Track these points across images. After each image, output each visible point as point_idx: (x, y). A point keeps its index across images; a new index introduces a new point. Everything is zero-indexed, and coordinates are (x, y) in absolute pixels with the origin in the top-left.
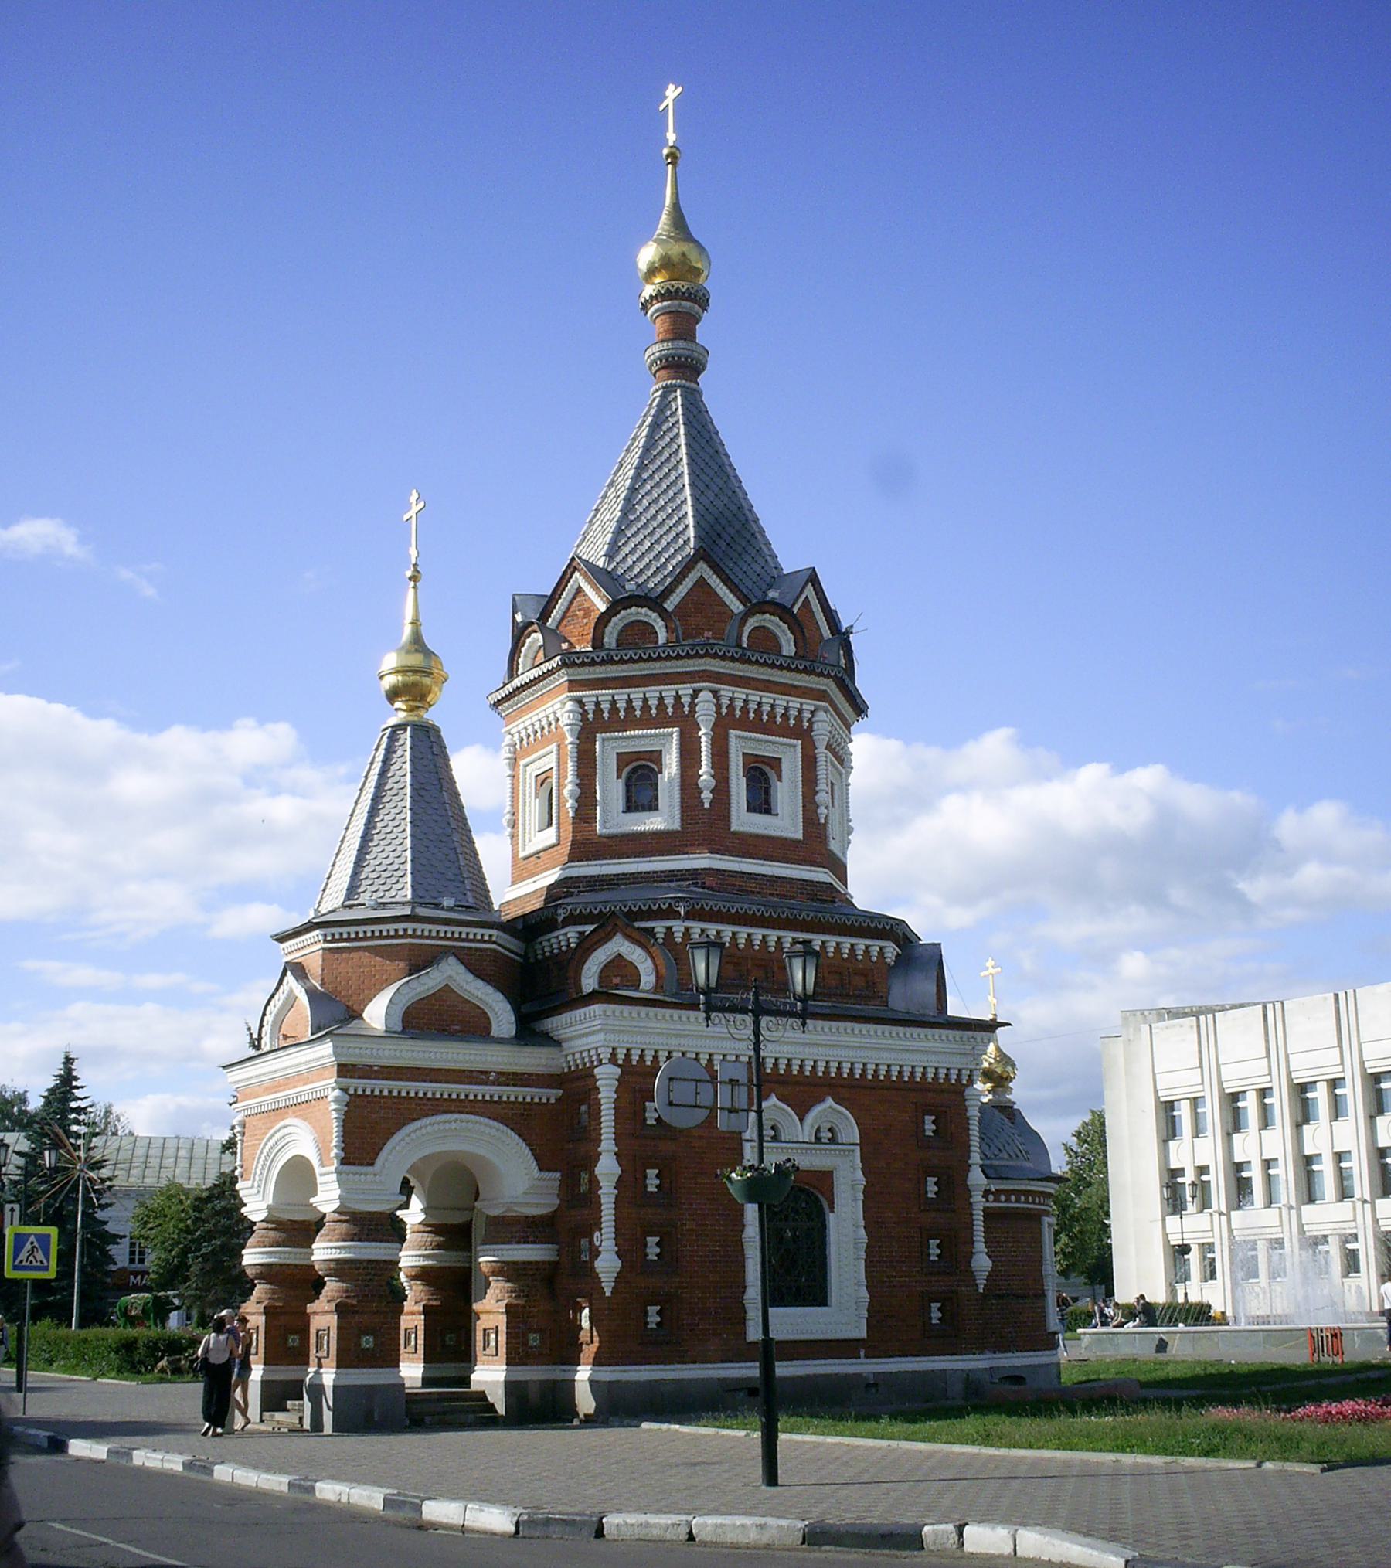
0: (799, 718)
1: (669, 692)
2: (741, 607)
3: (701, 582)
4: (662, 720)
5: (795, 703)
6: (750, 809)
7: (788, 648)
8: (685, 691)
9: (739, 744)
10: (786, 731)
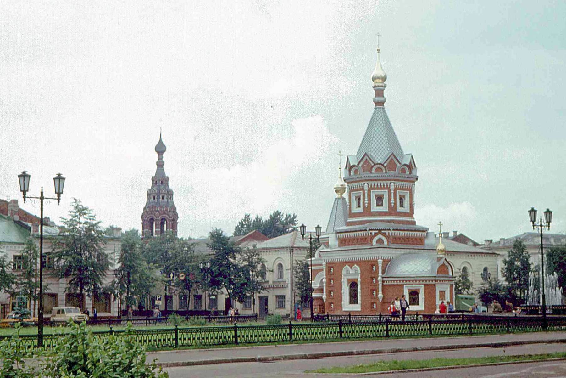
0: (387, 185)
4: (361, 190)
5: (385, 183)
6: (377, 205)
8: (363, 183)
10: (384, 188)
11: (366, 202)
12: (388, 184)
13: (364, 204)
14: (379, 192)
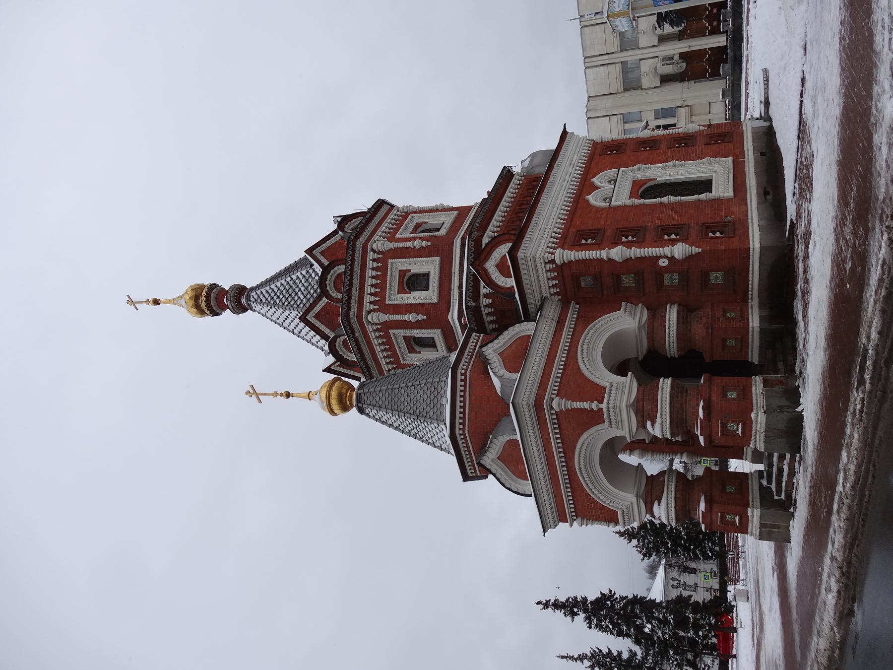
1: (372, 335)
2: (324, 299)
3: (317, 316)
4: (387, 336)
5: (370, 264)
7: (341, 268)
8: (369, 328)
9: (395, 298)
10: (383, 270)
11: (411, 317)
12: (376, 256)
13: (418, 325)
14: (393, 280)
